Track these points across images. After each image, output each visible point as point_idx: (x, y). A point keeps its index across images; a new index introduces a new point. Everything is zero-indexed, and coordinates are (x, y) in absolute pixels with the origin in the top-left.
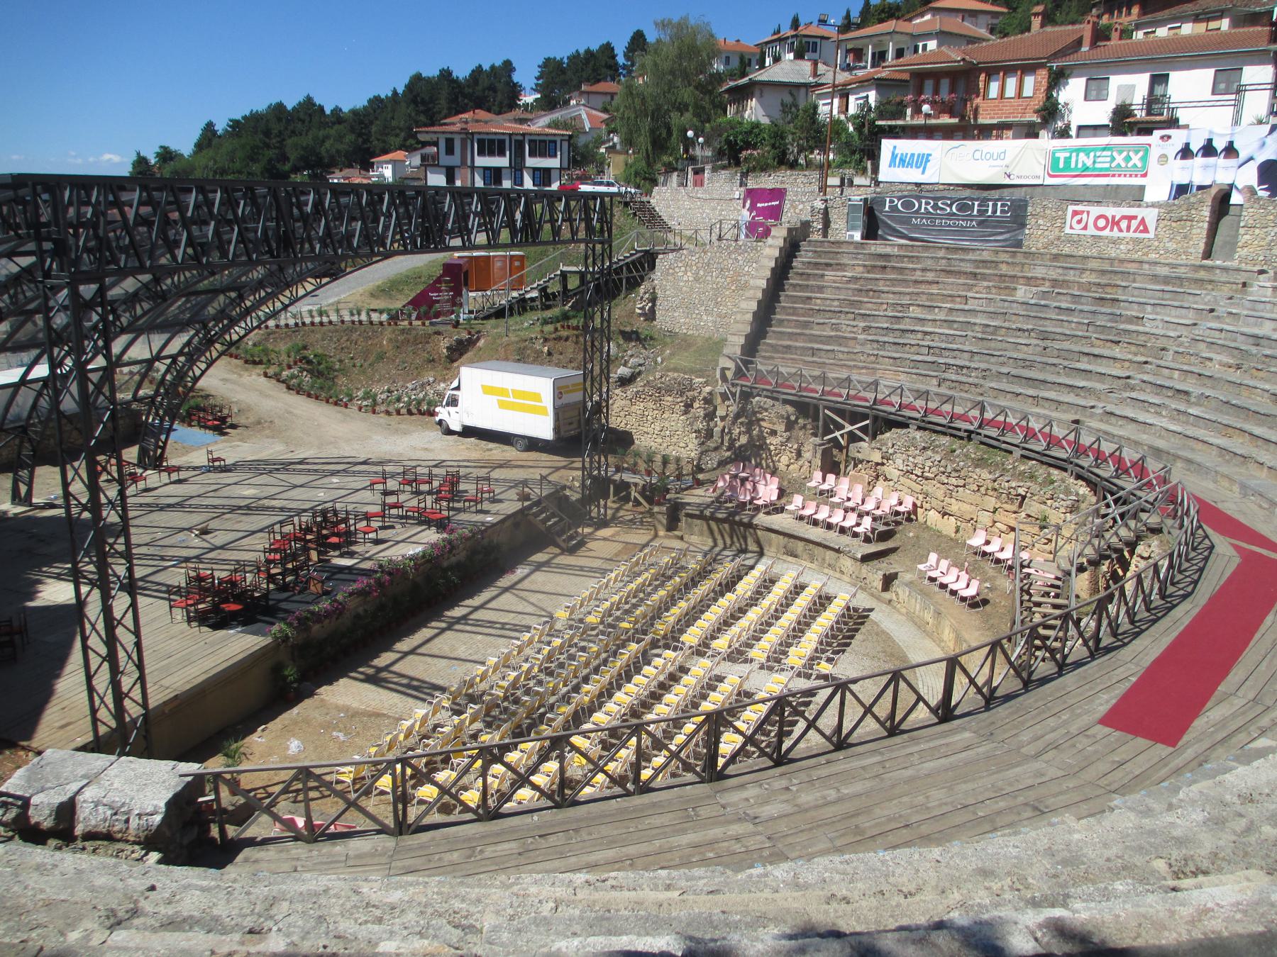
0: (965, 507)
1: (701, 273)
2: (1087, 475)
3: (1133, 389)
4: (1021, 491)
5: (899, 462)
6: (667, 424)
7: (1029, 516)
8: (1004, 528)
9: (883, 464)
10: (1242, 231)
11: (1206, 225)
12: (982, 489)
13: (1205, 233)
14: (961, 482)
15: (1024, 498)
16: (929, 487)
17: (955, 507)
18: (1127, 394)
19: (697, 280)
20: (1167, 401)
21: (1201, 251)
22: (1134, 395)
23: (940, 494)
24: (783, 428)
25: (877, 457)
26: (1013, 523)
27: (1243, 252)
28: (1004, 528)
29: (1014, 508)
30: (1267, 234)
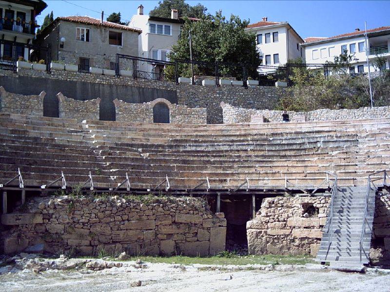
4: (172, 210)
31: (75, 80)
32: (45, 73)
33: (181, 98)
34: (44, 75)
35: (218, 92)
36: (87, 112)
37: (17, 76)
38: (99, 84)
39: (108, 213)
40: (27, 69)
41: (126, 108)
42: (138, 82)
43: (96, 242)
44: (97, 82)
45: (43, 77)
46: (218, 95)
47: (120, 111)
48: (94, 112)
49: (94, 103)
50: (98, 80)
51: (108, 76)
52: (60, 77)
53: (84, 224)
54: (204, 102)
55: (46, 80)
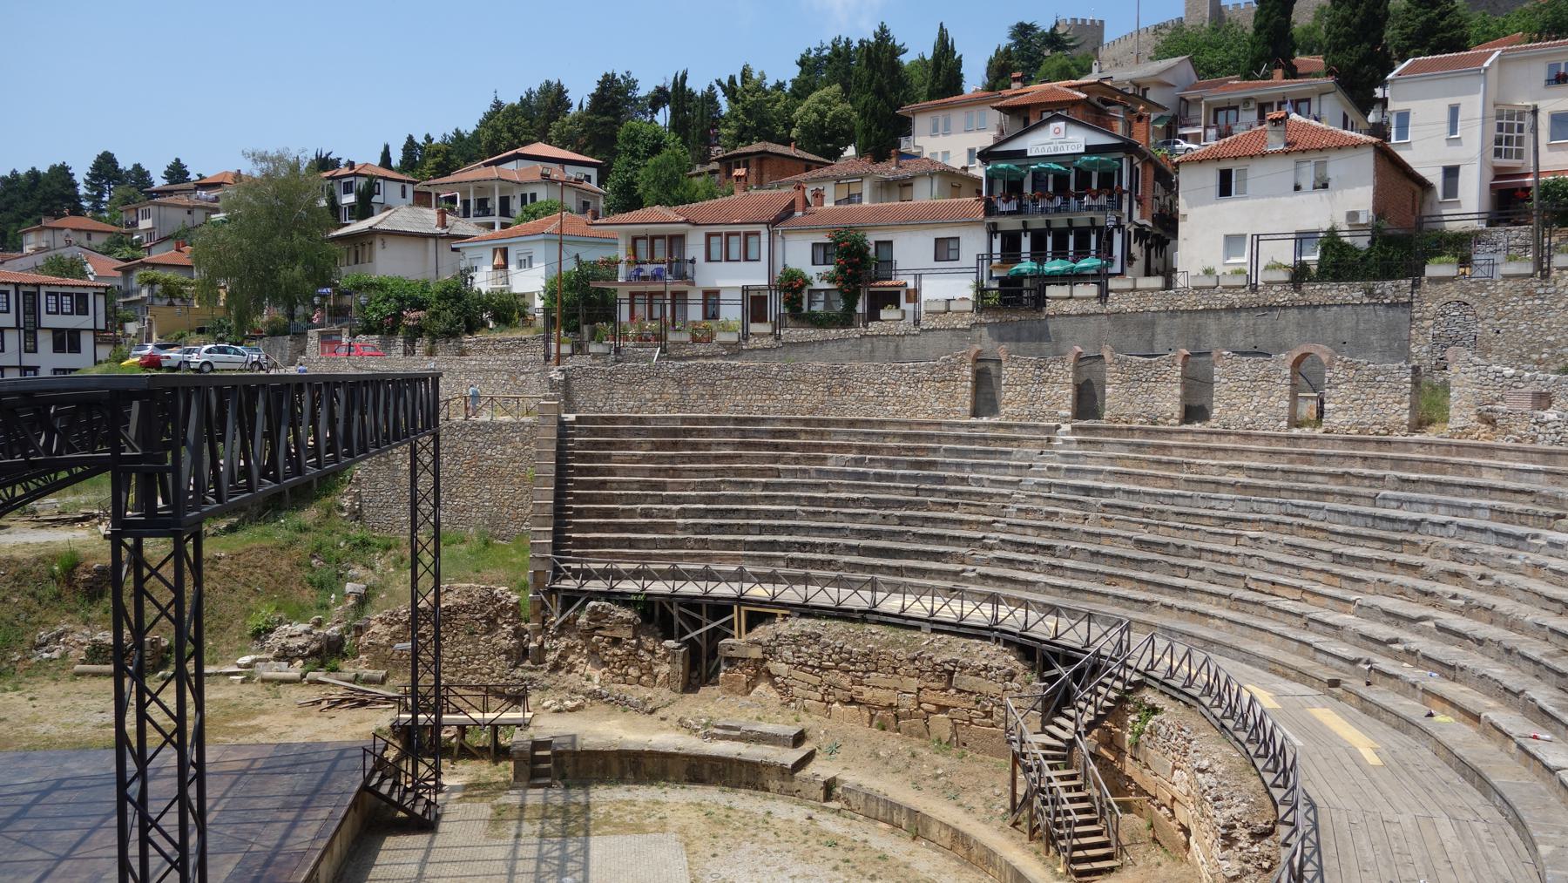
0: (880, 693)
2: (1017, 640)
4: (947, 666)
5: (788, 654)
7: (960, 691)
8: (933, 708)
9: (765, 660)
12: (901, 671)
13: (969, 391)
14: (872, 666)
15: (951, 673)
16: (830, 677)
18: (991, 555)
20: (1038, 558)
22: (998, 553)
24: (629, 633)
25: (756, 653)
28: (933, 708)
29: (942, 685)
30: (1028, 391)
33: (1421, 319)
34: (1094, 307)
35: (1541, 291)
46: (1537, 302)
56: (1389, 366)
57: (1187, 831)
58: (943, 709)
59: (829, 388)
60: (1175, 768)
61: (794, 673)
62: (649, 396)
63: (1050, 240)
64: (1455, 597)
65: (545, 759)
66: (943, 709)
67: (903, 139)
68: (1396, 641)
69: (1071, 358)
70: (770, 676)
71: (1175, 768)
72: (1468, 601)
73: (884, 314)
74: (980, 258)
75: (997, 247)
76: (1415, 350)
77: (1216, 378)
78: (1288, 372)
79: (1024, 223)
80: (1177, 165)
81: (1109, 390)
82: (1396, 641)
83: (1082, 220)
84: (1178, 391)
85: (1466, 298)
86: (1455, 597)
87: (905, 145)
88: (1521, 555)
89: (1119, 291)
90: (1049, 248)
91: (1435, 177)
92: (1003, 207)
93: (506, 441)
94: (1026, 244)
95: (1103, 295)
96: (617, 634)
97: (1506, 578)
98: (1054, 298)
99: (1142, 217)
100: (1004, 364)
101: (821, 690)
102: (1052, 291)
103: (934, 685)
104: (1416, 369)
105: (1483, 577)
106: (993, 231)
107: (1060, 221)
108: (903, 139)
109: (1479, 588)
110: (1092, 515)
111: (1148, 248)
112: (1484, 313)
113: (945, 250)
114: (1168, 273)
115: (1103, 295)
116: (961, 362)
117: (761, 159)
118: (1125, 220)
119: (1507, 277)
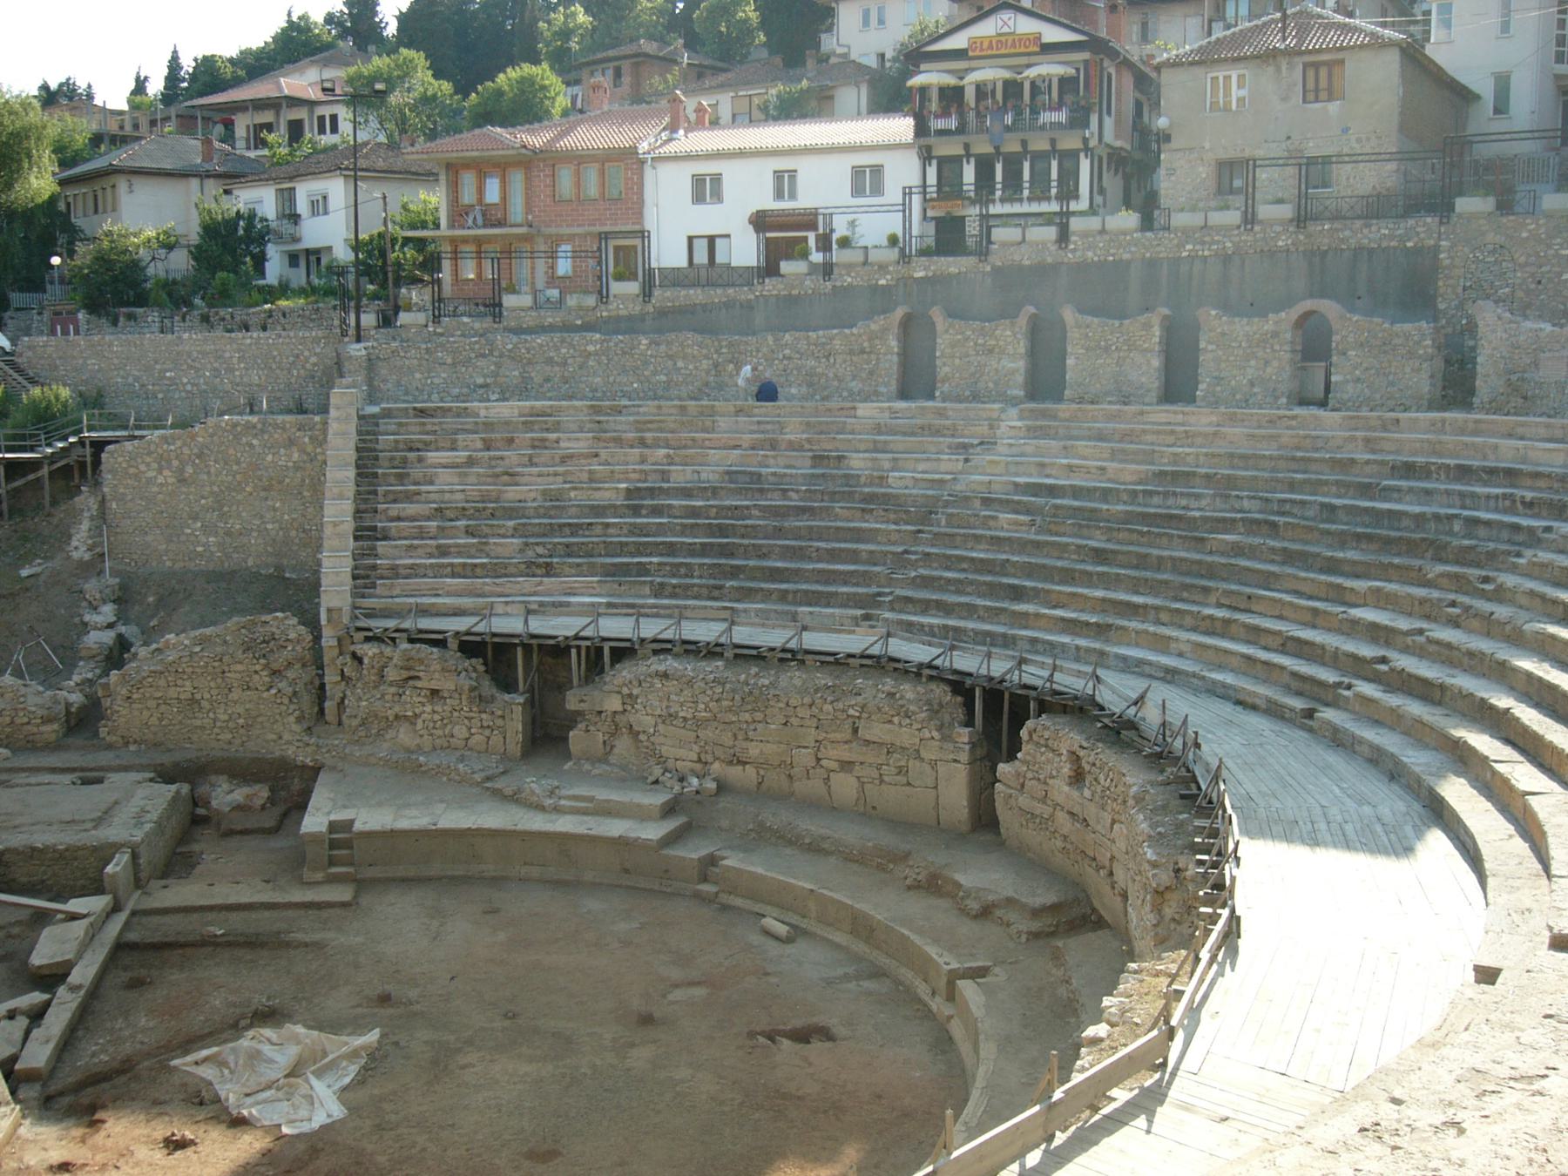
1: (189, 470)
3: (914, 565)
4: (851, 712)
6: (240, 709)
8: (834, 765)
10: (938, 362)
11: (895, 359)
14: (758, 716)
16: (707, 734)
17: (754, 750)
19: (182, 481)
21: (894, 386)
23: (727, 739)
25: (614, 704)
26: (847, 756)
27: (946, 387)
28: (834, 765)
31: (1126, 256)
32: (1053, 248)
34: (1052, 255)
36: (1130, 350)
37: (988, 268)
38: (1192, 258)
39: (725, 703)
40: (1012, 244)
41: (1223, 334)
42: (1309, 236)
43: (710, 758)
44: (1185, 254)
45: (1049, 260)
47: (1209, 342)
48: (1146, 350)
49: (1147, 326)
50: (1189, 247)
51: (1220, 229)
52: (1090, 254)
53: (685, 719)
54: (1533, 275)
55: (1055, 267)
56: (1407, 327)
57: (1124, 896)
58: (846, 766)
59: (716, 365)
60: (1114, 822)
61: (661, 727)
62: (480, 381)
63: (999, 168)
64: (1453, 604)
65: (347, 844)
66: (846, 766)
67: (823, 36)
68: (1384, 660)
69: (1022, 322)
70: (634, 734)
71: (1114, 822)
72: (1467, 609)
73: (786, 267)
74: (907, 192)
75: (932, 178)
76: (1442, 306)
77: (1202, 345)
78: (1288, 336)
79: (967, 146)
80: (1158, 68)
81: (1070, 362)
82: (1384, 660)
83: (1040, 144)
84: (1156, 363)
85: (1500, 239)
86: (1453, 604)
87: (828, 43)
88: (1528, 553)
89: (1085, 235)
90: (999, 177)
91: (1484, 87)
92: (940, 124)
93: (291, 442)
94: (969, 174)
95: (1064, 236)
96: (434, 685)
97: (1509, 580)
98: (1004, 245)
99: (1117, 137)
100: (940, 327)
101: (696, 748)
102: (999, 234)
103: (838, 736)
104: (1437, 330)
105: (1486, 580)
106: (926, 156)
107: (1013, 146)
108: (823, 36)
109: (1483, 595)
110: (1039, 519)
111: (1127, 179)
112: (1522, 260)
113: (867, 180)
114: (1149, 209)
115: (1064, 236)
116: (885, 330)
117: (636, 65)
118: (1093, 143)
119: (1549, 216)
